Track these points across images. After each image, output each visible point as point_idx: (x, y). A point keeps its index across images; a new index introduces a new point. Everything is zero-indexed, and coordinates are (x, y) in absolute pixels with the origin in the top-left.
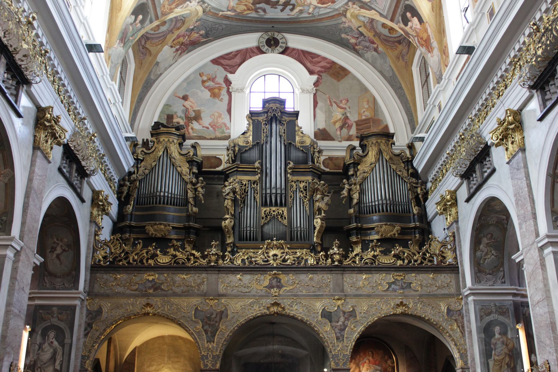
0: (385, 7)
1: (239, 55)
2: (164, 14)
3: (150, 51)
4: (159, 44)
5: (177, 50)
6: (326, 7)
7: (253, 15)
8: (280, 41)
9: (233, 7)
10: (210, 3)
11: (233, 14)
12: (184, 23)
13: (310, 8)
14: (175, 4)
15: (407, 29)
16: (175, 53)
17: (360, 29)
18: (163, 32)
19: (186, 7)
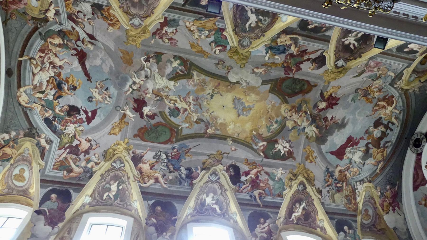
0: (400, 64)
1: (418, 170)
2: (356, 210)
3: (383, 229)
4: (381, 222)
5: (394, 210)
6: (397, 102)
7: (389, 150)
8: (419, 137)
9: (376, 162)
10: (365, 176)
11: (382, 163)
12: (373, 198)
13: (395, 112)
14: (352, 200)
15: (421, 51)
16: (396, 212)
17: (422, 81)
18: (373, 213)
19: (360, 193)
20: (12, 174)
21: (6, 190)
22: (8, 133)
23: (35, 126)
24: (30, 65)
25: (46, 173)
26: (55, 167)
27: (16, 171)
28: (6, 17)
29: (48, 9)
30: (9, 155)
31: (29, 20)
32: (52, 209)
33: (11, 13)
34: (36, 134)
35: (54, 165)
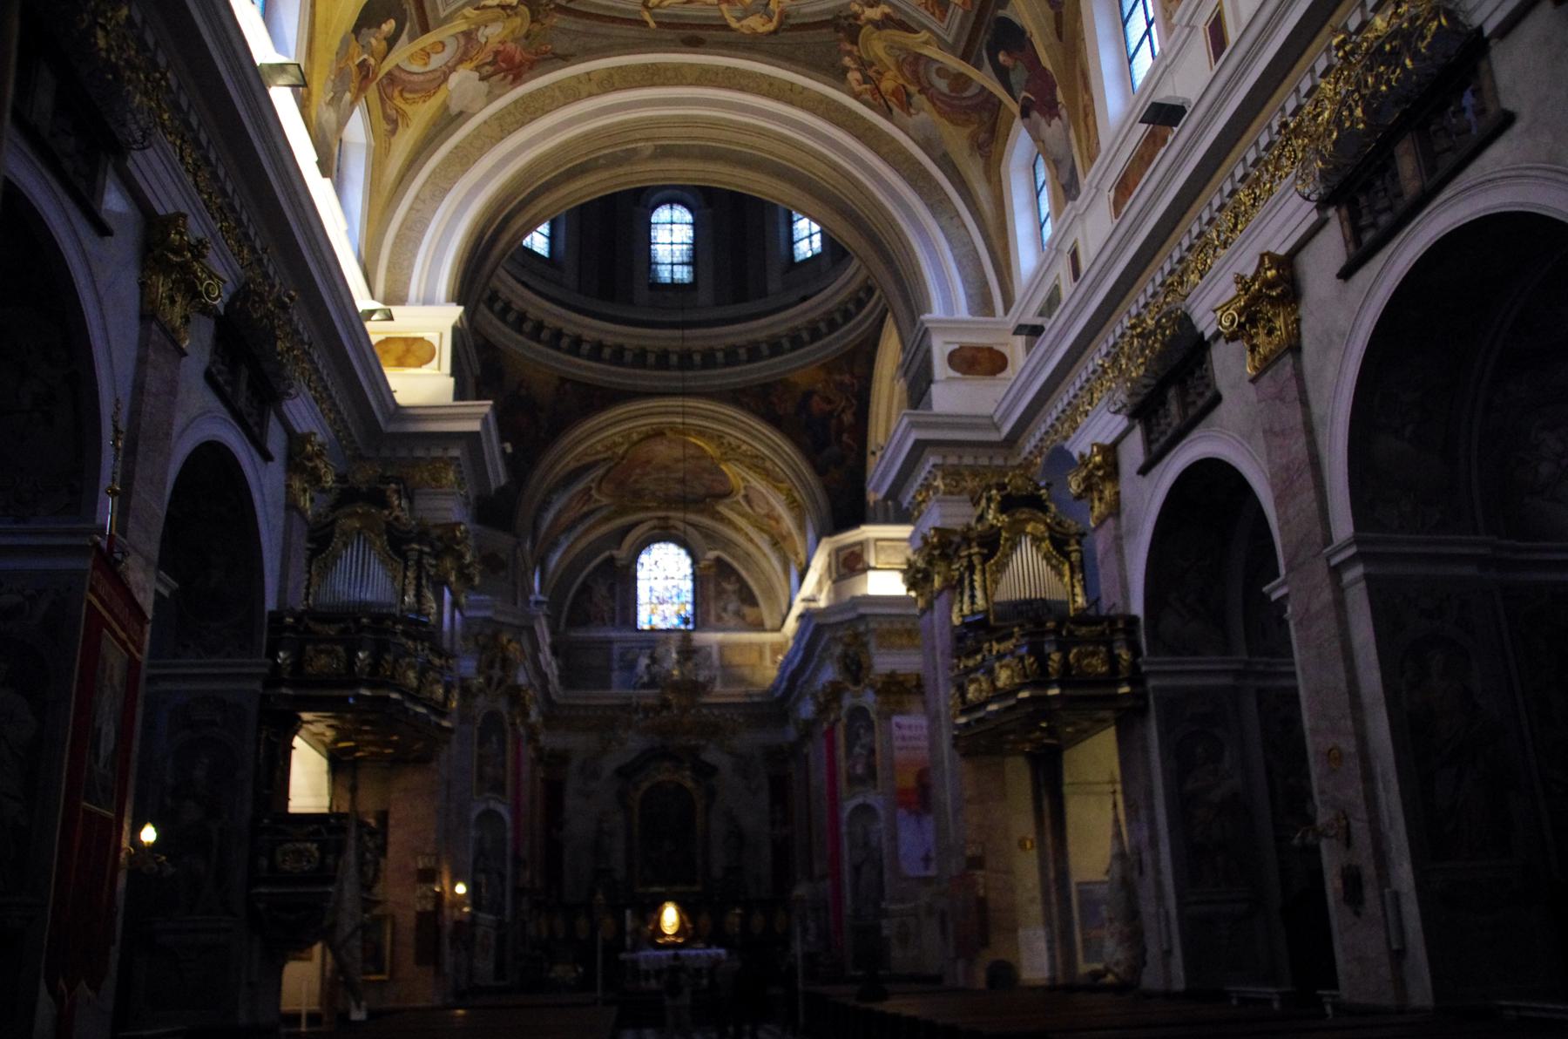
20: (944, 95)
21: (986, 116)
22: (846, 70)
23: (829, 17)
24: (665, 8)
25: (950, 40)
26: (937, 12)
27: (942, 85)
28: (551, 59)
29: (498, 6)
30: (897, 88)
31: (542, 24)
32: (1028, 81)
33: (537, 54)
34: (851, 21)
35: (933, 14)
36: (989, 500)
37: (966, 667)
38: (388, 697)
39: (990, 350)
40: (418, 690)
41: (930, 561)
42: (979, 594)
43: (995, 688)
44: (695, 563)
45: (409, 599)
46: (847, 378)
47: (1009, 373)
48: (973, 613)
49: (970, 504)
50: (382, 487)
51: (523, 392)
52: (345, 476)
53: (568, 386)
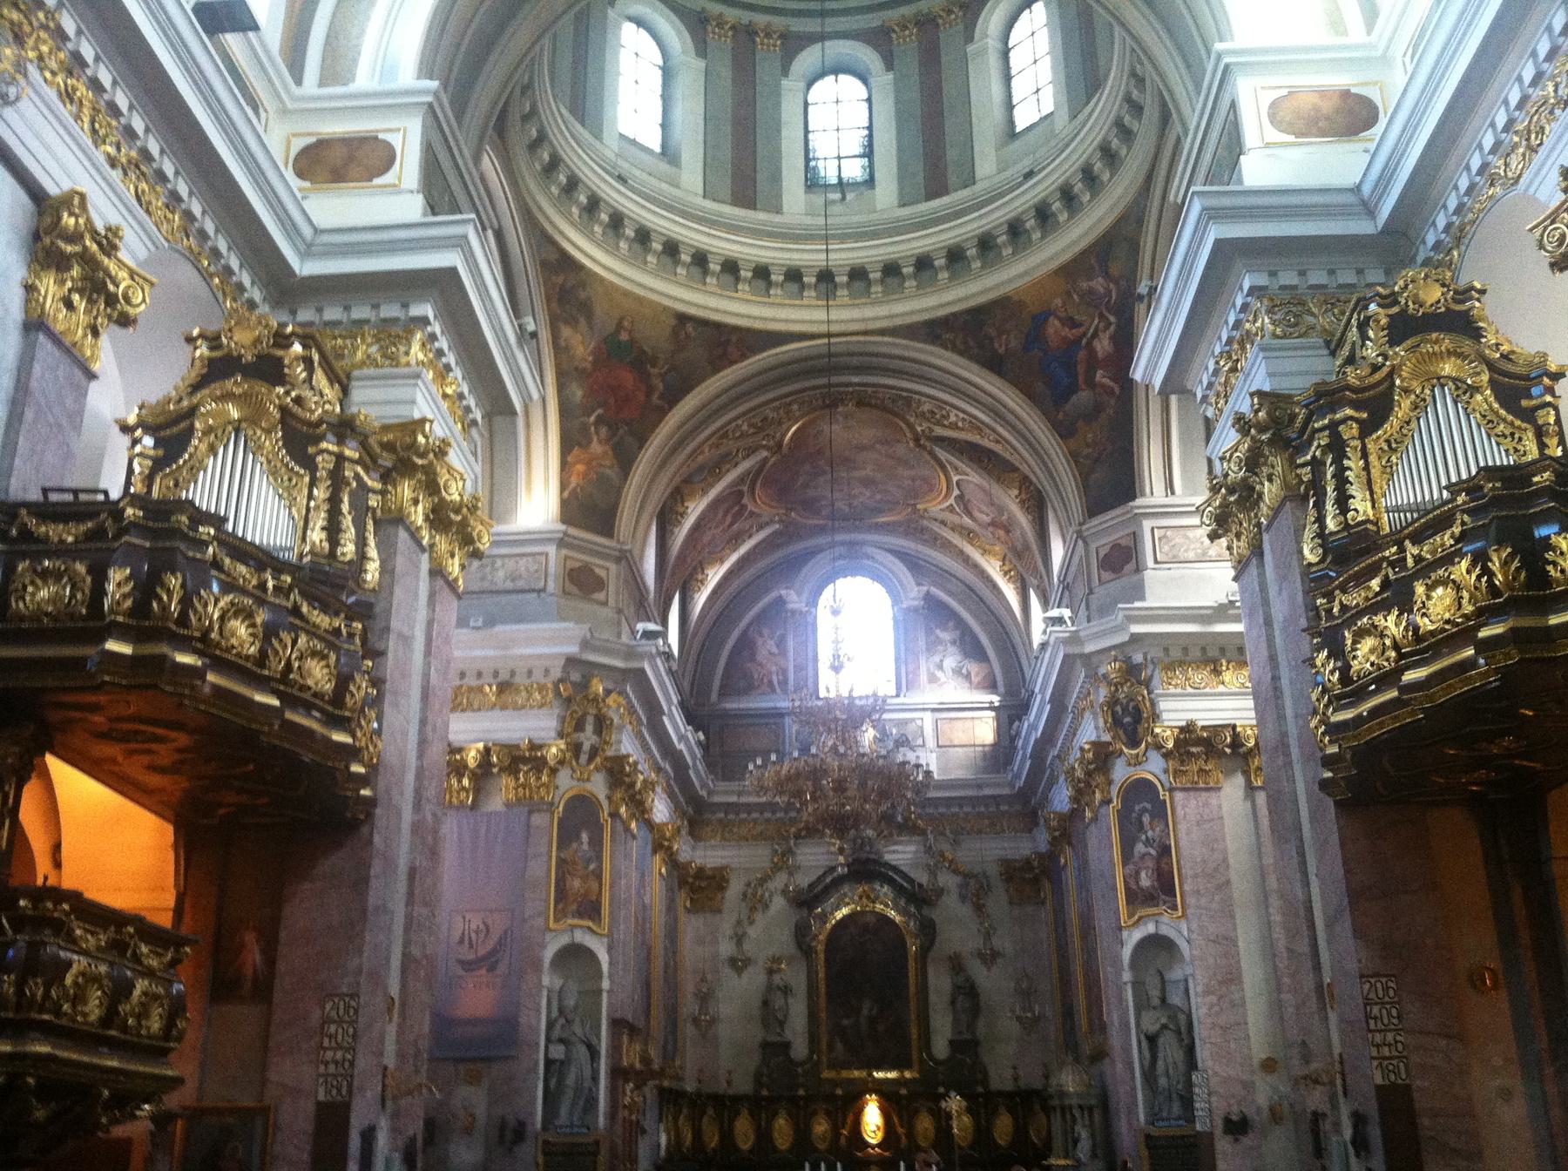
36: (1363, 326)
37: (1344, 608)
38: (163, 659)
39: (1346, 94)
40: (262, 658)
41: (1253, 462)
42: (1354, 490)
43: (1418, 636)
44: (896, 601)
45: (317, 536)
46: (1098, 284)
47: (1378, 129)
48: (1347, 526)
49: (1326, 352)
50: (280, 353)
51: (624, 337)
52: (219, 337)
53: (690, 328)
